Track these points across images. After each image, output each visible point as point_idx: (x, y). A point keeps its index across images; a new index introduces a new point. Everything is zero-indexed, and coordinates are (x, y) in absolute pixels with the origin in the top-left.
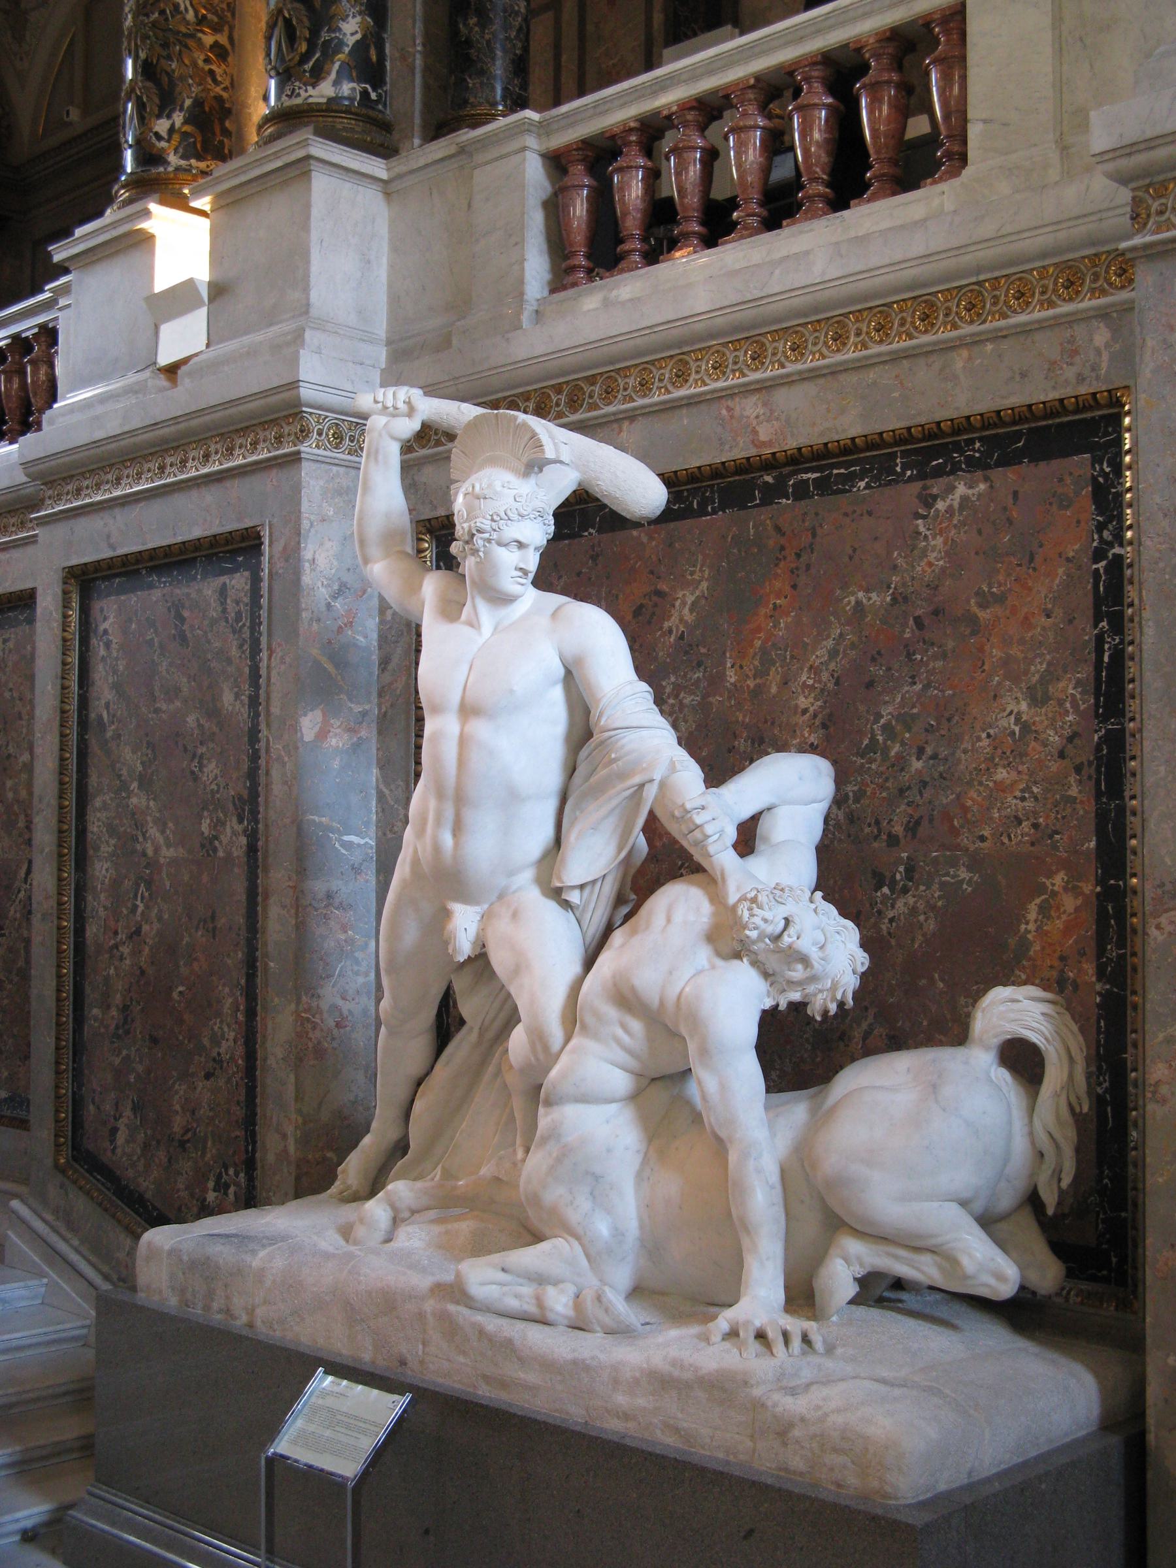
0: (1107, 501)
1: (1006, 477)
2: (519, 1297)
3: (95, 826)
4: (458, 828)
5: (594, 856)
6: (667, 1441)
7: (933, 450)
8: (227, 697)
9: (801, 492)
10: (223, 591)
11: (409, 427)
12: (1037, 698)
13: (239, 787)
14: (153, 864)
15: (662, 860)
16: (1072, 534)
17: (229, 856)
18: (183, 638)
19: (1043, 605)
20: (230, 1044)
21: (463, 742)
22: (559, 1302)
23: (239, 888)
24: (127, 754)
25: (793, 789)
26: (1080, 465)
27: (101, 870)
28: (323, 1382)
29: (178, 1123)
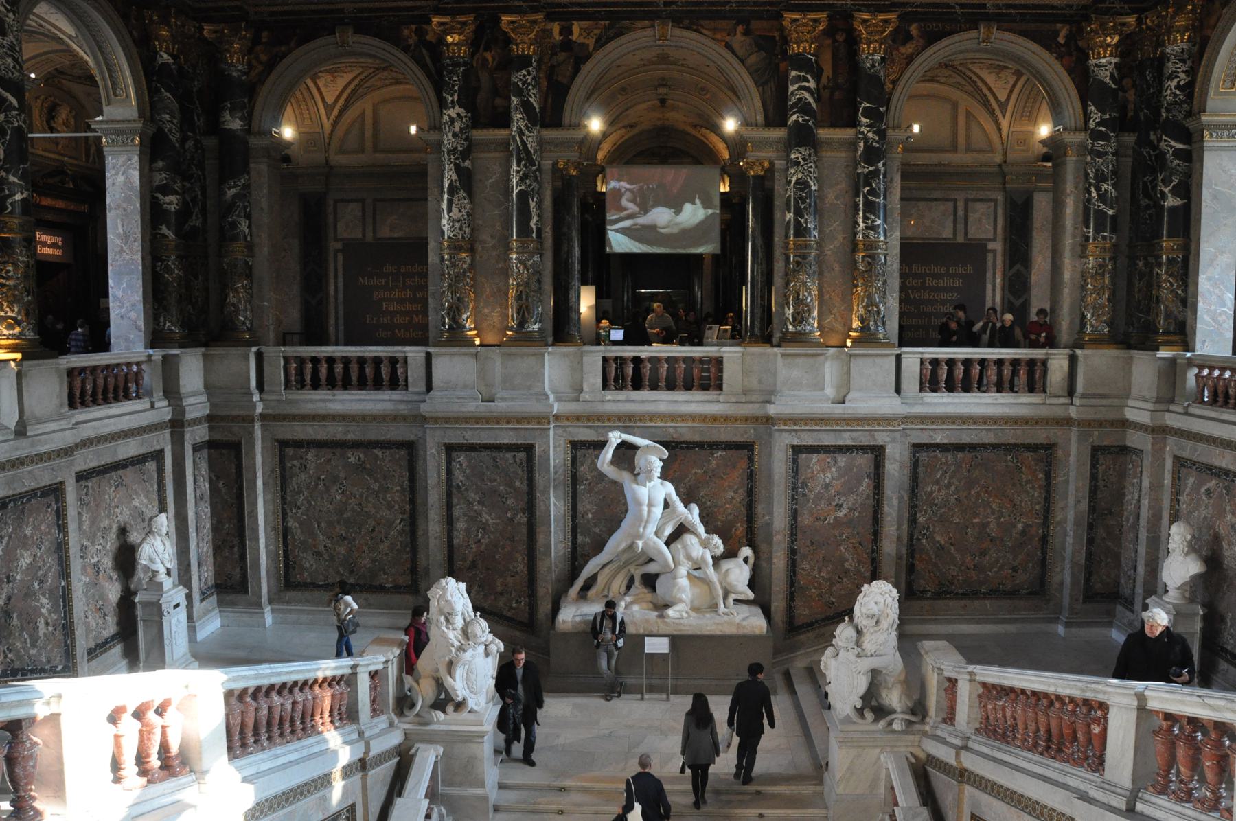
0: (751, 460)
1: (730, 452)
2: (677, 615)
3: (456, 513)
4: (645, 528)
5: (668, 531)
6: (718, 633)
7: (714, 446)
8: (518, 484)
9: (682, 448)
10: (514, 457)
11: (619, 441)
12: (735, 492)
13: (522, 505)
14: (486, 524)
15: (681, 530)
16: (744, 464)
17: (519, 523)
18: (497, 467)
19: (737, 476)
20: (521, 567)
21: (649, 512)
22: (685, 615)
23: (524, 531)
24: (472, 495)
25: (695, 509)
26: (745, 452)
27: (461, 525)
28: (646, 639)
29: (499, 589)
